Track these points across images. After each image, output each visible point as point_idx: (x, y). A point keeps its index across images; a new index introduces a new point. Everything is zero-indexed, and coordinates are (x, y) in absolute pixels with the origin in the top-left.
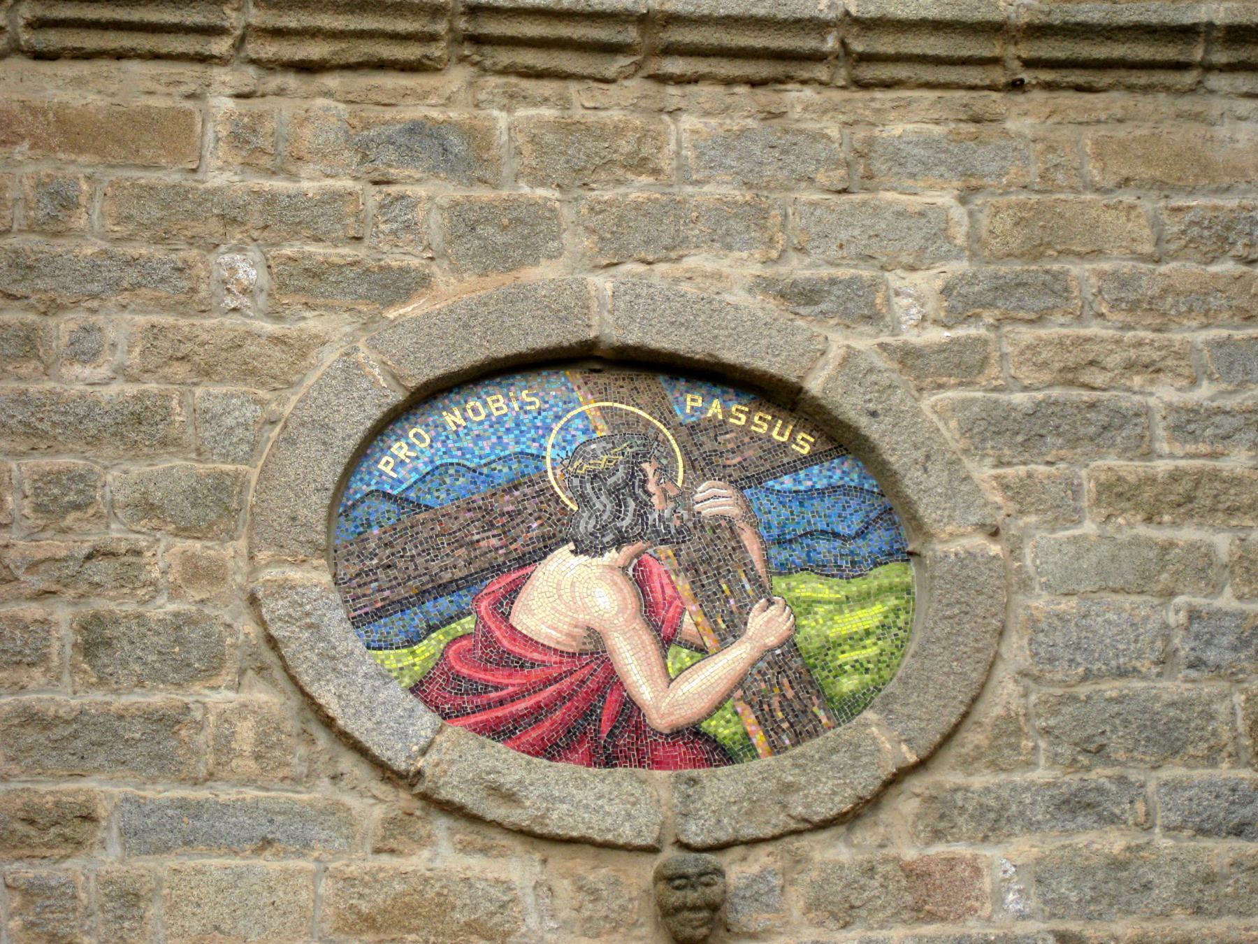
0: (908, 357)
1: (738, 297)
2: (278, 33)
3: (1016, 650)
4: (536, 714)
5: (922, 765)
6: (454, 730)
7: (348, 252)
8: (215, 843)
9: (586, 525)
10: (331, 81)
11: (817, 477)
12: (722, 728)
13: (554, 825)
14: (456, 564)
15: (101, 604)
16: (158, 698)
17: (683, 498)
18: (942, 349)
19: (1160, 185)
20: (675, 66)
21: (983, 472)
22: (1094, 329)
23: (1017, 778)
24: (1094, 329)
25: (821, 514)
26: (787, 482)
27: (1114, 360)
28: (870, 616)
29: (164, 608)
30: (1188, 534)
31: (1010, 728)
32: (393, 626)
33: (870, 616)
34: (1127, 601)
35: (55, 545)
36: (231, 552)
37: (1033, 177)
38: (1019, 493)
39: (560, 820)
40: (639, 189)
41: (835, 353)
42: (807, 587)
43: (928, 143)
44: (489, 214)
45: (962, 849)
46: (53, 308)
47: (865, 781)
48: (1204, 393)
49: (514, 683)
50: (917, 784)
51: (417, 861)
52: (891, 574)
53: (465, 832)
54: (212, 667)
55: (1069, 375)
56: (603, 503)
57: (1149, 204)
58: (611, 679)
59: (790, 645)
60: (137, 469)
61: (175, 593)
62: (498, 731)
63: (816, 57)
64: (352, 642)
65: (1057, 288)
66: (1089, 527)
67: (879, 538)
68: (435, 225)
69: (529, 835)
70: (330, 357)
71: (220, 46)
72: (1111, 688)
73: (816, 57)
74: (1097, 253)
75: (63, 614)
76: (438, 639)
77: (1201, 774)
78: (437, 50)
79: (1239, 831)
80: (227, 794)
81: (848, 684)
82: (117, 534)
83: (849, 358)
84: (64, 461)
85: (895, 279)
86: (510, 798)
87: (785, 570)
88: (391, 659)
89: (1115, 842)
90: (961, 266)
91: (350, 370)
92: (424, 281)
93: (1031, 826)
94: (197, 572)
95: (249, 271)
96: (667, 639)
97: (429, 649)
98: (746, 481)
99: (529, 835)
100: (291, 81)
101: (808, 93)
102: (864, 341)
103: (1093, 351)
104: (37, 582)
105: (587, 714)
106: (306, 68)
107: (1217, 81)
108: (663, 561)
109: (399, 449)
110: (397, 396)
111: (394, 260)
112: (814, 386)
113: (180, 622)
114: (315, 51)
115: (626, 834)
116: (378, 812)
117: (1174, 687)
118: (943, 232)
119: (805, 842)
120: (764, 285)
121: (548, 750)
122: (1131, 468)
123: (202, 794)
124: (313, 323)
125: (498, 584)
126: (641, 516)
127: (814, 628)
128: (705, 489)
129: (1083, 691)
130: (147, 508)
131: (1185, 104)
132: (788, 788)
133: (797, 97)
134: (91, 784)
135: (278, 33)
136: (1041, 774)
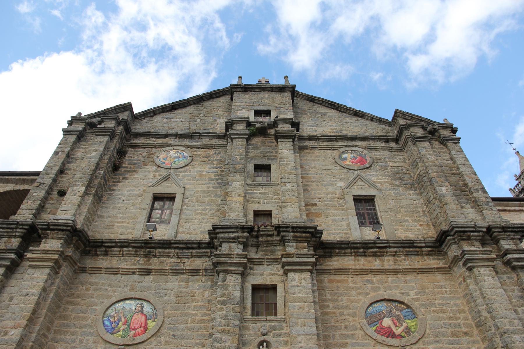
0: (413, 299)
1: (397, 294)
2: (354, 272)
3: (428, 326)
4: (385, 333)
5: (421, 338)
6: (379, 335)
7: (363, 291)
9: (387, 315)
10: (359, 276)
11: (407, 310)
12: (402, 334)
13: (389, 344)
14: (376, 319)
15: (346, 324)
16: (352, 332)
17: (395, 313)
18: (416, 298)
19: (432, 282)
20: (388, 273)
21: (422, 310)
22: (429, 296)
23: (430, 339)
24: (429, 296)
25: (408, 314)
26: (404, 311)
27: (432, 298)
28: (414, 323)
29: (352, 324)
30: (441, 315)
31: (429, 334)
32: (372, 325)
33: (414, 323)
34: (437, 322)
35: (341, 318)
36: (357, 318)
37: (421, 282)
38: (425, 311)
40: (387, 285)
41: (407, 299)
42: (408, 321)
43: (411, 279)
44: (374, 287)
45: (426, 346)
46: (338, 297)
47: (417, 340)
48: (440, 301)
49: (383, 330)
50: (421, 340)
52: (415, 319)
53: (381, 345)
54: (356, 330)
55: (428, 300)
56: (388, 313)
57: (432, 284)
58: (392, 330)
59: (407, 326)
60: (348, 311)
61: (352, 323)
62: (382, 335)
63: (400, 272)
64: (368, 327)
65: (425, 292)
66: (432, 315)
67: (413, 316)
69: (387, 345)
70: (363, 301)
71: (350, 273)
72: (437, 330)
73: (400, 272)
74: (428, 289)
75: (343, 324)
76: (376, 327)
77: (447, 338)
78: (368, 273)
79: (452, 344)
80: (359, 341)
81: (413, 330)
82: (347, 317)
83: (408, 299)
84: (341, 311)
85: (411, 292)
86: (385, 341)
87: (405, 319)
88: (372, 328)
89: (441, 345)
90: (416, 290)
91: (365, 302)
92: (370, 293)
93: (432, 344)
94: (354, 321)
95: (355, 293)
96: (396, 326)
97: (375, 327)
98: (400, 311)
99: (387, 345)
100: (356, 276)
101: (400, 275)
102: (409, 297)
103: (429, 298)
104: (340, 322)
105: (390, 333)
106: (357, 275)
107: (435, 272)
108: (394, 319)
109: (370, 309)
110: (369, 304)
111: (367, 292)
112: (405, 302)
113: (353, 325)
114: (358, 273)
115: (396, 345)
116: (373, 343)
117: (443, 330)
118: (414, 287)
119: (412, 346)
120: (399, 293)
121: (386, 337)
122: (435, 309)
123: (357, 341)
124: (360, 298)
125: (380, 321)
126: (392, 315)
127: (409, 325)
128: (397, 312)
129: (435, 330)
130: (349, 315)
131: (433, 275)
132: (410, 340)
133: (399, 276)
134: (348, 340)
135: (354, 272)
136: (432, 339)
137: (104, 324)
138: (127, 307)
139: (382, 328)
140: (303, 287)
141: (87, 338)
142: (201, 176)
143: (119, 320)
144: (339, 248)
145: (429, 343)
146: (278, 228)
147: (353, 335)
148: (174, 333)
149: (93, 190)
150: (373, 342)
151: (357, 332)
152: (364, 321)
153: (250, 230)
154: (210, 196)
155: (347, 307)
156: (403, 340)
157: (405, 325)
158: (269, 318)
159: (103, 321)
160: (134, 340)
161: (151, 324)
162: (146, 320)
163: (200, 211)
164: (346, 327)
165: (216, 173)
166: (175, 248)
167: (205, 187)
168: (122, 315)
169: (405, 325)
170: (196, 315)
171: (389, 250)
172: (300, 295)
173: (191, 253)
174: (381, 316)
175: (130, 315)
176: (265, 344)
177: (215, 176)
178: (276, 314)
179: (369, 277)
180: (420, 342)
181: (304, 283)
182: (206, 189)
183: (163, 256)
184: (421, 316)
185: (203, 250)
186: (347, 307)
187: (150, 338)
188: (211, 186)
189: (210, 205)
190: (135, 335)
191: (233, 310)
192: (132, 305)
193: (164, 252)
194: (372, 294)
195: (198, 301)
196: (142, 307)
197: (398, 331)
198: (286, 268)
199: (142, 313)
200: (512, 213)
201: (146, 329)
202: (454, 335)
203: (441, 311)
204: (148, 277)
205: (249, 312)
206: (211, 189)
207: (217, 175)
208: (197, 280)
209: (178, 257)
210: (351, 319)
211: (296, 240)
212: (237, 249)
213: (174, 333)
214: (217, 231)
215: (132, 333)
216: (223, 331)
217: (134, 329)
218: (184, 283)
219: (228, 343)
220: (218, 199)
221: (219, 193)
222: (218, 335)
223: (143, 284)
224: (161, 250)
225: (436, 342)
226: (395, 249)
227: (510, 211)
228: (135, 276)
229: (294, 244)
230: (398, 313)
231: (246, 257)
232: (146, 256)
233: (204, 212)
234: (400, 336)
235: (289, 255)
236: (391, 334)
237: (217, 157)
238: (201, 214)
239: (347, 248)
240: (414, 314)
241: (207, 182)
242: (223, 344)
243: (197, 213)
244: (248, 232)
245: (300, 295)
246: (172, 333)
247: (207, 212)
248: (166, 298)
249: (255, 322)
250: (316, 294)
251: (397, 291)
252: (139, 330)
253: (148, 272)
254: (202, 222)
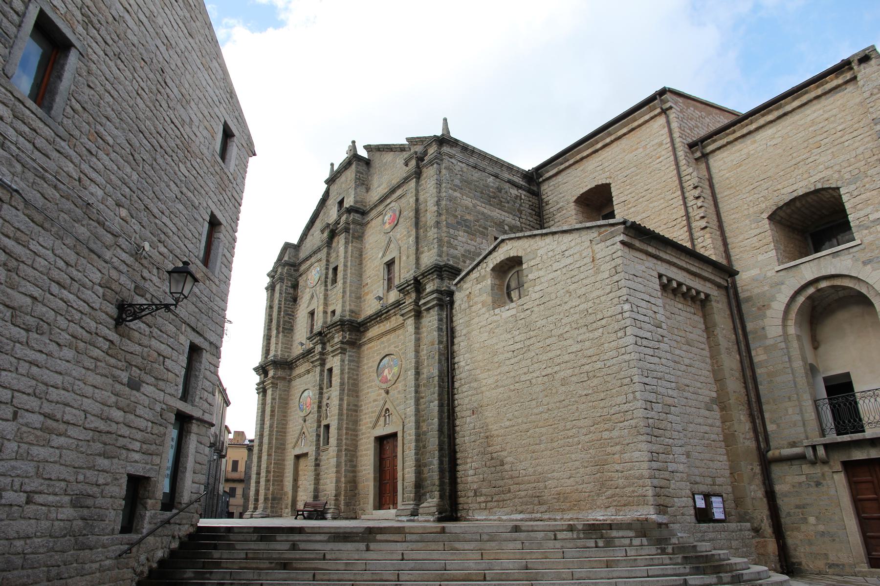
144: (369, 322)
149: (281, 329)
171: (391, 312)
200: (644, 127)
226: (393, 311)
227: (639, 126)
239: (376, 318)
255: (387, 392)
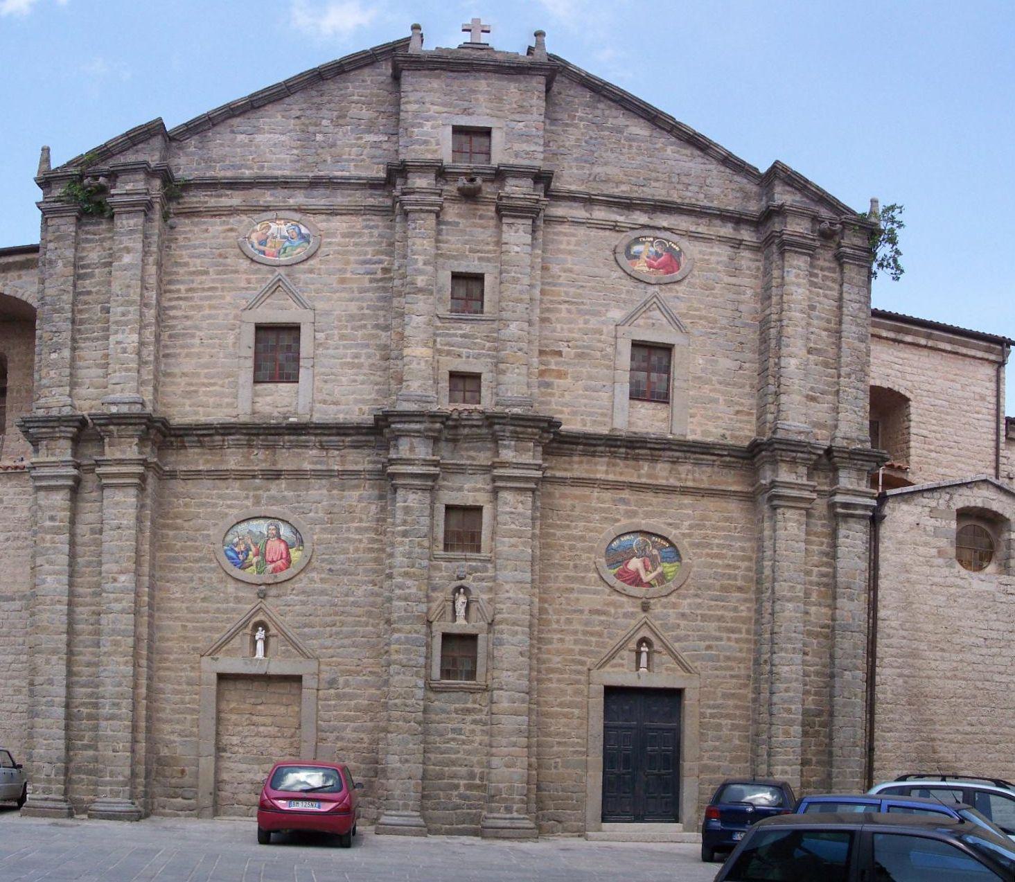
0: (683, 534)
8: (589, 593)
11: (669, 550)
14: (620, 559)
16: (582, 575)
39: (631, 594)
42: (665, 564)
44: (630, 511)
47: (670, 591)
51: (613, 597)
52: (677, 563)
58: (639, 575)
62: (624, 581)
64: (607, 569)
68: (622, 512)
89: (700, 601)
99: (628, 596)
102: (678, 531)
117: (711, 581)
120: (665, 523)
121: (630, 584)
122: (710, 551)
124: (605, 526)
127: (666, 570)
130: (582, 549)
137: (226, 554)
138: (254, 530)
139: (626, 572)
140: (519, 514)
141: (209, 575)
142: (342, 281)
143: (248, 550)
145: (685, 597)
146: (490, 420)
147: (583, 578)
148: (331, 566)
150: (607, 590)
151: (590, 575)
152: (603, 560)
153: (444, 418)
154: (365, 326)
155: (582, 538)
156: (652, 589)
157: (659, 569)
158: (469, 555)
159: (225, 551)
160: (276, 577)
161: (295, 555)
162: (288, 547)
163: (349, 360)
164: (575, 567)
165: (372, 274)
166: (316, 435)
167: (353, 308)
168: (249, 542)
169: (659, 569)
170: (361, 541)
172: (513, 526)
173: (343, 441)
174: (629, 554)
175: (262, 541)
176: (462, 590)
177: (371, 281)
178: (478, 549)
179: (626, 494)
180: (674, 594)
181: (520, 508)
182: (355, 311)
183: (296, 447)
184: (685, 560)
185: (363, 438)
186: (582, 538)
187: (298, 574)
188: (365, 305)
189: (367, 346)
190: (275, 570)
191: (420, 545)
192: (262, 527)
193: (297, 441)
194: (624, 521)
195: (361, 520)
196: (278, 529)
197: (646, 577)
198: (497, 484)
199: (279, 538)
201: (289, 561)
202: (724, 589)
203: (717, 556)
204: (277, 482)
205: (441, 546)
206: (366, 312)
207: (377, 281)
208: (357, 487)
209: (322, 447)
210: (584, 556)
211: (517, 437)
212: (422, 451)
213: (331, 566)
214: (390, 419)
215: (270, 567)
216: (406, 574)
217: (273, 562)
218: (335, 492)
219: (414, 590)
220: (380, 332)
221: (381, 321)
222: (400, 580)
223: (273, 492)
224: (292, 438)
225: (697, 596)
228: (257, 481)
229: (513, 443)
230: (655, 552)
231: (436, 464)
232: (267, 447)
233: (356, 361)
234: (649, 584)
235: (503, 465)
236: (636, 580)
237: (372, 236)
238: (352, 366)
240: (678, 556)
241: (357, 295)
242: (407, 591)
243: (345, 363)
244: (442, 423)
245: (513, 526)
246: (329, 567)
247: (362, 360)
248: (311, 514)
249: (449, 560)
250: (538, 523)
251: (662, 520)
252: (279, 563)
253: (276, 475)
254: (355, 381)
255: (645, 608)
